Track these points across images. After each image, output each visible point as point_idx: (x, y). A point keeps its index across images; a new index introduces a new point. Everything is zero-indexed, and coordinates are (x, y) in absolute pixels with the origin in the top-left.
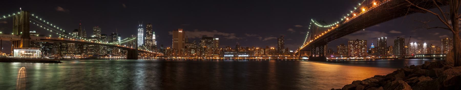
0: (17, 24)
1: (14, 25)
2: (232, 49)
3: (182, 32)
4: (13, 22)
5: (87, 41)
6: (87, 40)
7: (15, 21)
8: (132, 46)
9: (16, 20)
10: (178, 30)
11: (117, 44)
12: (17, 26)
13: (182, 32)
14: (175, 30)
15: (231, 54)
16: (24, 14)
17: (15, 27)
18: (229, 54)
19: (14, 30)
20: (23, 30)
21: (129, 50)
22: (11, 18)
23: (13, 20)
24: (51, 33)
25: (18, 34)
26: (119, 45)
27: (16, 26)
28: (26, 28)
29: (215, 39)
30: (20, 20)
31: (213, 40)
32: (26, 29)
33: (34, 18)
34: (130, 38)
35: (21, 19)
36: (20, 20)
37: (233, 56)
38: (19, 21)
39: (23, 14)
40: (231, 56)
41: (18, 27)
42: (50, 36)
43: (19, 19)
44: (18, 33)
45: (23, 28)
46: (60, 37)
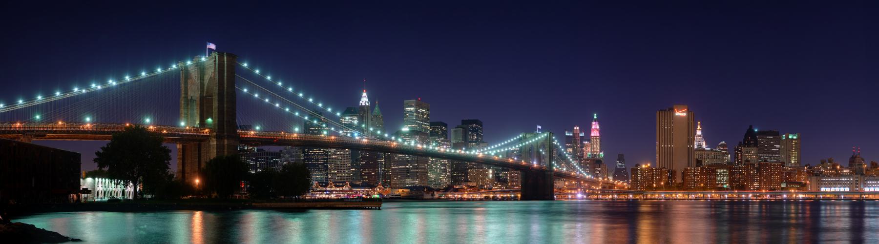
0: (194, 93)
1: (183, 95)
2: (841, 167)
3: (684, 114)
4: (182, 86)
5: (406, 146)
6: (406, 143)
7: (186, 83)
8: (535, 160)
9: (189, 81)
10: (672, 110)
11: (493, 154)
12: (193, 98)
13: (684, 114)
14: (665, 110)
15: (844, 185)
16: (217, 62)
17: (189, 102)
18: (835, 184)
19: (183, 111)
20: (215, 110)
21: (526, 171)
22: (176, 75)
23: (182, 81)
24: (298, 121)
25: (201, 124)
26: (498, 157)
27: (189, 98)
28: (225, 105)
29: (787, 138)
30: (206, 82)
31: (780, 138)
32: (225, 109)
33: (249, 74)
34: (528, 136)
35: (207, 78)
36: (203, 80)
37: (847, 189)
38: (202, 85)
39: (215, 61)
40: (842, 189)
41: (198, 100)
42: (297, 129)
43: (202, 79)
44: (198, 122)
45: (215, 104)
46: (325, 133)
